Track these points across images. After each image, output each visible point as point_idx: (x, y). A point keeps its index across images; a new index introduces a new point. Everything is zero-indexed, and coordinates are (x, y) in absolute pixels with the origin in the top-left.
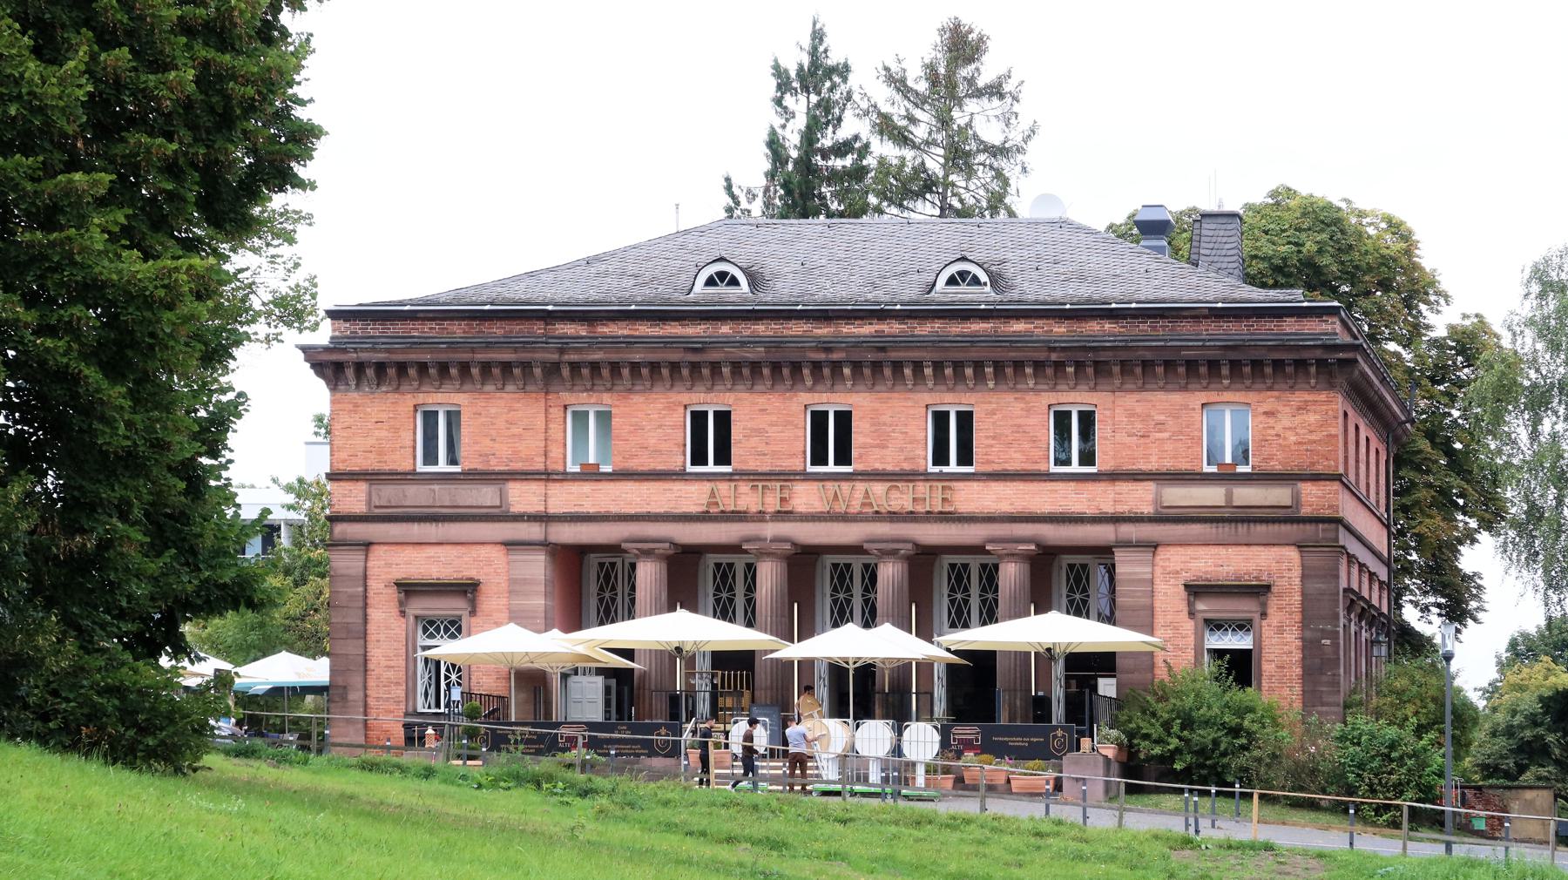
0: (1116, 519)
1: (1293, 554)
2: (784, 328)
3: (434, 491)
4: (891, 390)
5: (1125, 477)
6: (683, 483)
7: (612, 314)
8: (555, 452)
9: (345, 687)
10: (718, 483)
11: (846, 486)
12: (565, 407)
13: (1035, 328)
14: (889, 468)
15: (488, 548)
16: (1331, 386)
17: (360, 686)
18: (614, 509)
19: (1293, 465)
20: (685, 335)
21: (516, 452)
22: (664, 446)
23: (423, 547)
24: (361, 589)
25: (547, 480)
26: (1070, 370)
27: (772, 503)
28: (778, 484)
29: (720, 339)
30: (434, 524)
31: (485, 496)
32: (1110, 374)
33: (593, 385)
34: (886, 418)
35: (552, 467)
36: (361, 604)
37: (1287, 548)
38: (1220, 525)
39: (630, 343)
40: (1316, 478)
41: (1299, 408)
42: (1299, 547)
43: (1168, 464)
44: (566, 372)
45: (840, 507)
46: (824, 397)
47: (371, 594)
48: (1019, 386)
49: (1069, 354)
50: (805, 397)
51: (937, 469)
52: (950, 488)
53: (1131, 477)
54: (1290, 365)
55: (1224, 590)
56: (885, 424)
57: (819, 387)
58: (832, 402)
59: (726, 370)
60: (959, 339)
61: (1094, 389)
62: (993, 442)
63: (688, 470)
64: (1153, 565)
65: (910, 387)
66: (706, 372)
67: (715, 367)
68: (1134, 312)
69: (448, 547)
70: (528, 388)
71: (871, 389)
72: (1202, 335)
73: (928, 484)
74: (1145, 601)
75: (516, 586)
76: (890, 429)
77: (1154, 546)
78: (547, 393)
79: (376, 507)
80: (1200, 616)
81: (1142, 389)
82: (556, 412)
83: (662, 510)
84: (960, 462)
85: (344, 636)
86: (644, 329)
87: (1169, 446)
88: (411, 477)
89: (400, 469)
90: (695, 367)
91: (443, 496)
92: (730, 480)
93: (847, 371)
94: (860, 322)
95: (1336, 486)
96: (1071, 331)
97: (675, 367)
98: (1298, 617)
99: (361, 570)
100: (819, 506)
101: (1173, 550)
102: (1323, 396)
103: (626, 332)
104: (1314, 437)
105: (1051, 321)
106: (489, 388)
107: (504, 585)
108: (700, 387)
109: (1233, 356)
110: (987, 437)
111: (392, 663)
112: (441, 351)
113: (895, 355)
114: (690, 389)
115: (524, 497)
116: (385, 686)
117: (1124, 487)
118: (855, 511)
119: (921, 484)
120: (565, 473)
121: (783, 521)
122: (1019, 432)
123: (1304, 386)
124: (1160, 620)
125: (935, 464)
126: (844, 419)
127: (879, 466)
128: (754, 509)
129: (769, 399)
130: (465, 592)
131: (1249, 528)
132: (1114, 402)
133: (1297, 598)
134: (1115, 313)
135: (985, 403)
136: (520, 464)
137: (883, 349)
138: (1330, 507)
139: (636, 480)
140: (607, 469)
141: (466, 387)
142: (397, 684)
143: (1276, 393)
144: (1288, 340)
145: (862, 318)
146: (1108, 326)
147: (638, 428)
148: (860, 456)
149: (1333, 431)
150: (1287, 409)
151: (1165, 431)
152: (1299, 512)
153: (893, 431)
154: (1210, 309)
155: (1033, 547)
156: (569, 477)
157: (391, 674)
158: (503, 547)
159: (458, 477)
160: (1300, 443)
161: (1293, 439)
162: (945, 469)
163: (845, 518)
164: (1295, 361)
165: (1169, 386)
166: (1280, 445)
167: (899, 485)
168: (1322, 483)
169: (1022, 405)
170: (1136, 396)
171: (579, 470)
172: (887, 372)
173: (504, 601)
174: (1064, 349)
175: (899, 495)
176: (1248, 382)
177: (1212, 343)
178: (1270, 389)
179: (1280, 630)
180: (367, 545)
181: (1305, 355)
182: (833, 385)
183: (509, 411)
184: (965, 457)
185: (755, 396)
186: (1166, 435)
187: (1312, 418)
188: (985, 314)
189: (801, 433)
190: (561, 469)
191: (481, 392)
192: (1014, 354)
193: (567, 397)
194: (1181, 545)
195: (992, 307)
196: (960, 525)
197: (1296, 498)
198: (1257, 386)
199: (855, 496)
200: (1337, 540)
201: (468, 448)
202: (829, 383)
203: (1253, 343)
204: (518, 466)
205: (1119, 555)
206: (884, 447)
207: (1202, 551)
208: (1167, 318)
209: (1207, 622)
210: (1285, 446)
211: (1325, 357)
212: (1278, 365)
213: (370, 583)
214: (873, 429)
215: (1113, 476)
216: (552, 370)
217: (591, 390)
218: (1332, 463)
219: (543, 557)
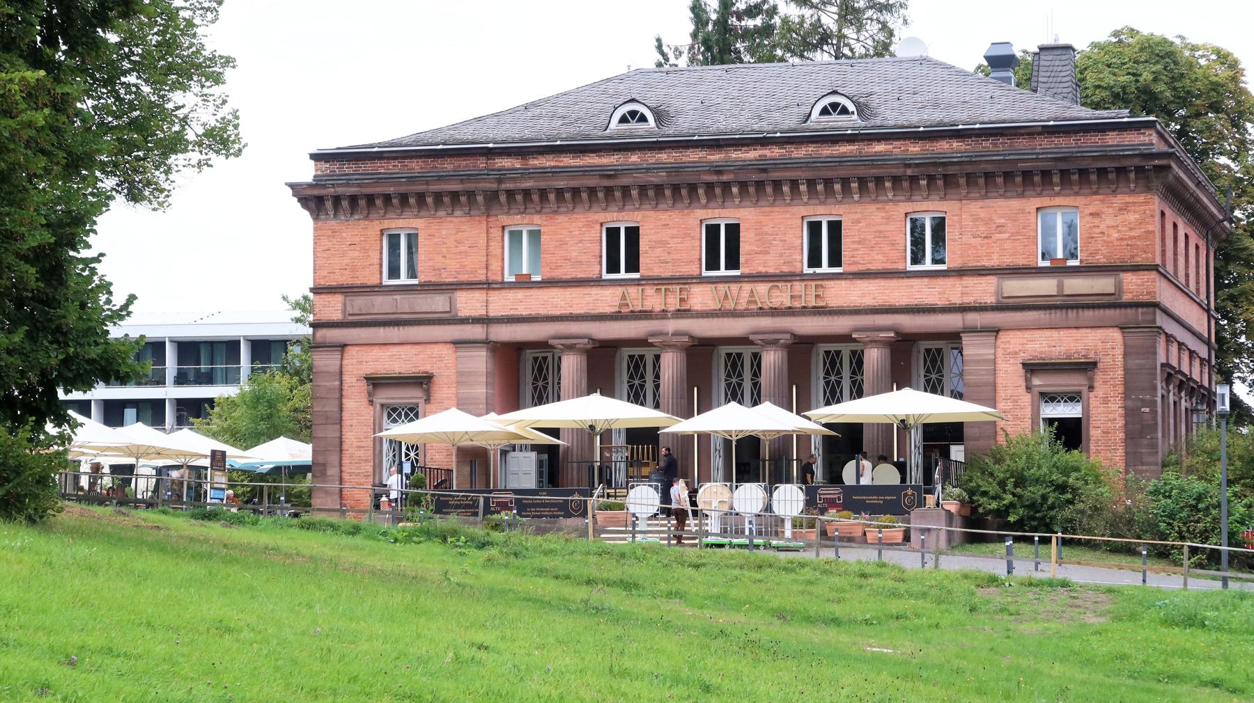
0: (963, 309)
1: (1116, 335)
2: (683, 156)
3: (396, 299)
4: (772, 205)
5: (970, 273)
6: (599, 288)
7: (541, 149)
8: (495, 265)
9: (324, 465)
10: (628, 288)
11: (734, 287)
12: (503, 228)
13: (894, 148)
14: (771, 270)
15: (440, 347)
16: (1148, 189)
17: (337, 463)
19: (1116, 258)
20: (600, 164)
21: (463, 266)
22: (584, 258)
23: (388, 347)
24: (337, 383)
25: (489, 289)
26: (923, 183)
27: (673, 303)
28: (678, 287)
29: (630, 167)
30: (396, 328)
31: (438, 303)
32: (958, 186)
33: (526, 208)
34: (768, 229)
35: (492, 278)
36: (337, 396)
37: (1111, 330)
38: (1053, 311)
39: (556, 172)
40: (1136, 268)
41: (1121, 209)
42: (1121, 328)
43: (1008, 261)
44: (503, 198)
45: (730, 305)
46: (717, 212)
47: (345, 387)
48: (880, 198)
49: (922, 169)
50: (700, 213)
51: (811, 271)
52: (822, 286)
53: (976, 272)
54: (1112, 172)
55: (1057, 367)
56: (767, 234)
57: (712, 204)
58: (722, 217)
59: (634, 193)
60: (829, 160)
61: (943, 198)
63: (604, 277)
64: (995, 348)
65: (788, 202)
66: (618, 194)
67: (626, 190)
68: (977, 132)
69: (409, 347)
70: (473, 212)
71: (756, 204)
72: (1035, 149)
73: (803, 284)
74: (991, 378)
75: (463, 378)
76: (772, 238)
77: (996, 331)
78: (488, 216)
79: (350, 315)
80: (1036, 390)
81: (985, 197)
82: (496, 232)
83: (582, 312)
84: (831, 265)
85: (324, 422)
86: (567, 161)
87: (1008, 245)
88: (378, 289)
89: (369, 283)
90: (609, 191)
91: (404, 304)
92: (638, 285)
93: (735, 190)
94: (746, 148)
95: (1153, 275)
96: (924, 150)
97: (592, 191)
98: (1121, 389)
99: (338, 367)
100: (712, 305)
101: (1012, 334)
102: (1141, 198)
103: (552, 164)
104: (1133, 234)
105: (907, 142)
106: (441, 213)
107: (453, 378)
108: (613, 207)
109: (1063, 166)
110: (854, 242)
111: (363, 444)
112: (400, 184)
113: (775, 175)
114: (605, 210)
115: (469, 303)
116: (357, 463)
117: (969, 281)
118: (743, 308)
119: (797, 283)
120: (503, 283)
121: (683, 318)
122: (880, 237)
123: (1125, 189)
124: (1001, 394)
125: (810, 266)
126: (733, 230)
127: (762, 269)
128: (658, 308)
129: (671, 216)
130: (422, 383)
131: (1077, 313)
132: (961, 209)
133: (1120, 372)
134: (962, 133)
136: (466, 276)
137: (765, 171)
138: (1148, 293)
139: (561, 287)
140: (537, 278)
141: (422, 213)
142: (367, 461)
143: (1101, 197)
144: (1110, 151)
145: (748, 145)
146: (956, 144)
147: (563, 243)
148: (747, 262)
149: (1150, 228)
150: (1111, 210)
151: (1005, 232)
152: (1121, 298)
154: (1043, 126)
155: (892, 335)
156: (506, 286)
157: (361, 453)
159: (416, 288)
160: (1122, 239)
161: (1116, 235)
162: (818, 270)
163: (734, 314)
164: (1116, 168)
165: (1009, 194)
166: (1105, 241)
167: (779, 284)
168: (1142, 273)
169: (884, 214)
170: (980, 203)
171: (514, 280)
172: (769, 189)
173: (453, 390)
174: (917, 165)
175: (779, 294)
176: (1076, 188)
177: (1044, 156)
178: (1096, 193)
179: (1106, 401)
180: (343, 347)
181: (1126, 163)
182: (724, 202)
183: (457, 232)
184: (835, 260)
185: (659, 213)
186: (1006, 236)
187: (1132, 217)
188: (851, 138)
189: (697, 243)
190: (499, 279)
191: (434, 217)
192: (875, 171)
193: (504, 219)
194: (1019, 329)
195: (857, 132)
196: (830, 318)
197: (1119, 286)
198: (1083, 191)
199: (742, 295)
200: (1154, 321)
201: (424, 264)
202: (720, 201)
203: (1079, 155)
204: (464, 278)
205: (966, 339)
206: (767, 253)
207: (1037, 334)
208: (1007, 136)
209: (1043, 395)
210: (1108, 242)
211: (1143, 164)
212: (1102, 172)
213: (345, 378)
214: (757, 238)
215: (960, 273)
216: (492, 197)
217: (523, 213)
218: (1150, 255)
219: (485, 353)
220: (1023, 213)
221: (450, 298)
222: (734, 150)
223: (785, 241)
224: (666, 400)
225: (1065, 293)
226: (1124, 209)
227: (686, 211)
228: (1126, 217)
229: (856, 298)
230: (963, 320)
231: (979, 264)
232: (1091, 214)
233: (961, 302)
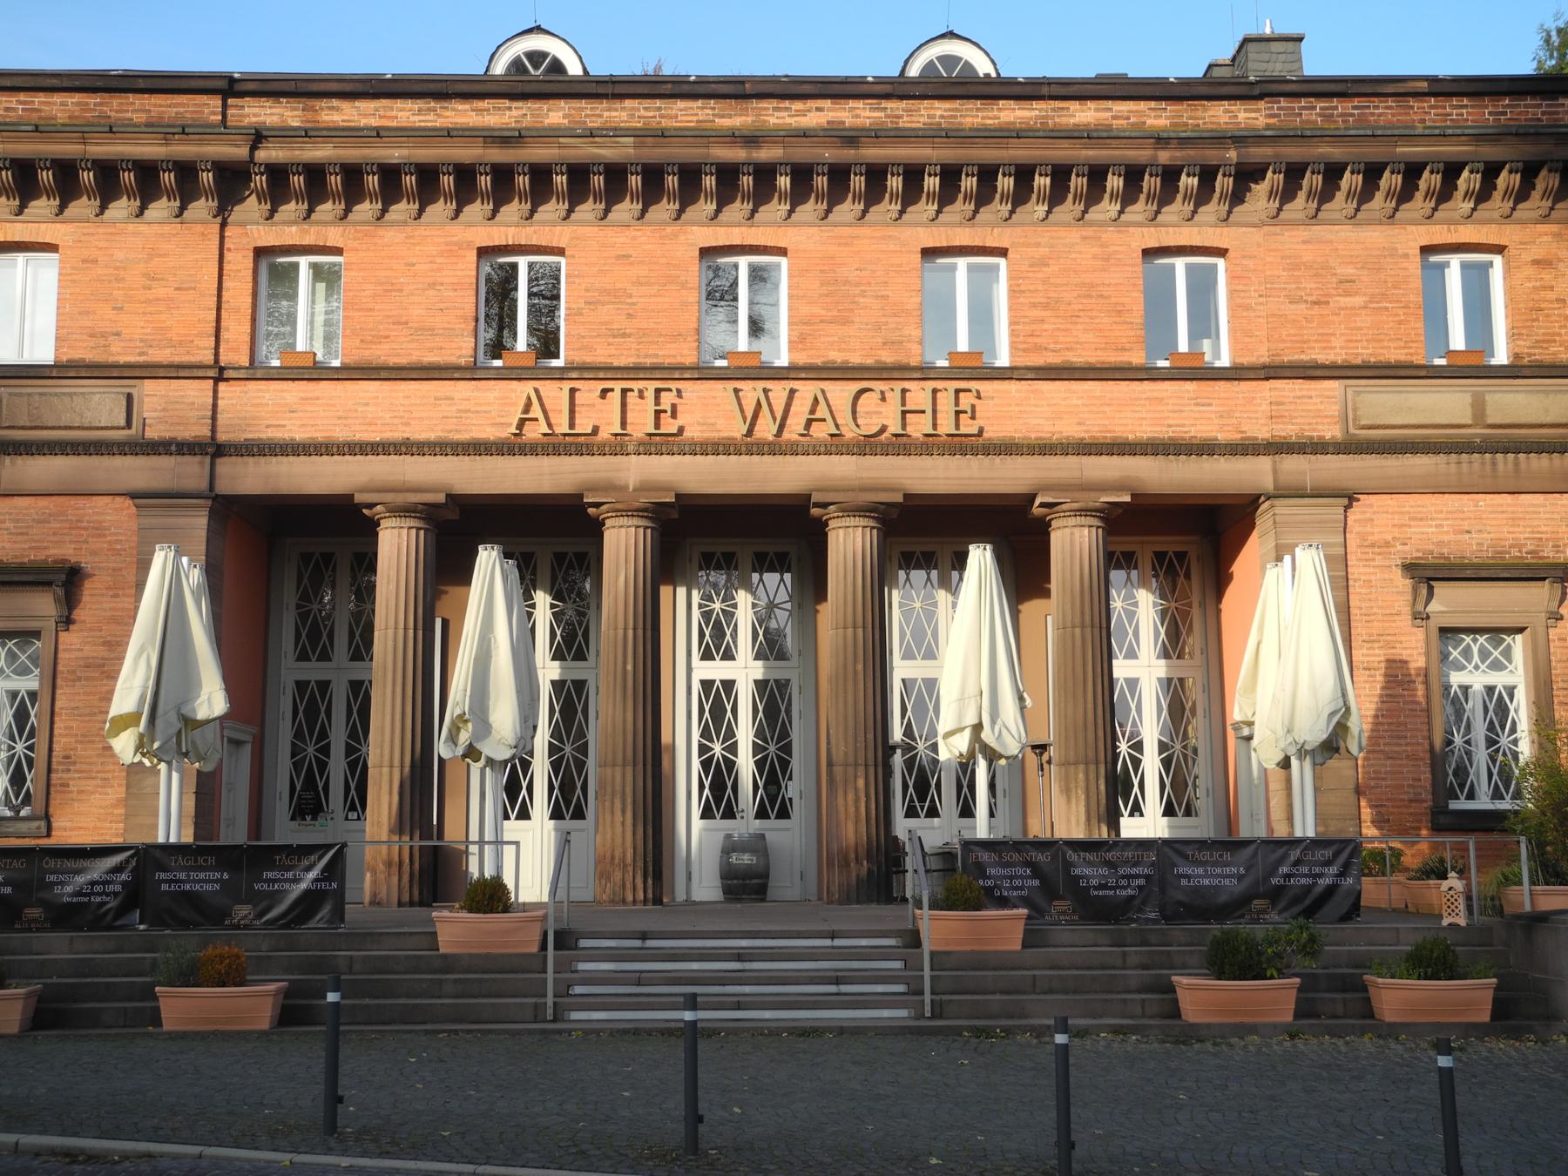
2: (662, 116)
14: (856, 359)
18: (341, 434)
43: (1364, 352)
56: (846, 282)
62: (1043, 313)
76: (857, 291)
80: (1435, 623)
83: (432, 436)
86: (405, 113)
110: (1034, 305)
122: (1090, 296)
127: (836, 357)
129: (634, 238)
135: (1028, 245)
136: (168, 351)
151: (1356, 294)
153: (863, 294)
158: (129, 502)
170: (1303, 233)
185: (609, 232)
186: (1358, 300)
206: (846, 322)
214: (824, 290)
220: (1391, 256)
221: (129, 398)
222: (775, 109)
223: (886, 297)
225: (1490, 421)
229: (1042, 422)
230: (1275, 471)
231: (1303, 357)
232: (1536, 262)
233: (1267, 435)
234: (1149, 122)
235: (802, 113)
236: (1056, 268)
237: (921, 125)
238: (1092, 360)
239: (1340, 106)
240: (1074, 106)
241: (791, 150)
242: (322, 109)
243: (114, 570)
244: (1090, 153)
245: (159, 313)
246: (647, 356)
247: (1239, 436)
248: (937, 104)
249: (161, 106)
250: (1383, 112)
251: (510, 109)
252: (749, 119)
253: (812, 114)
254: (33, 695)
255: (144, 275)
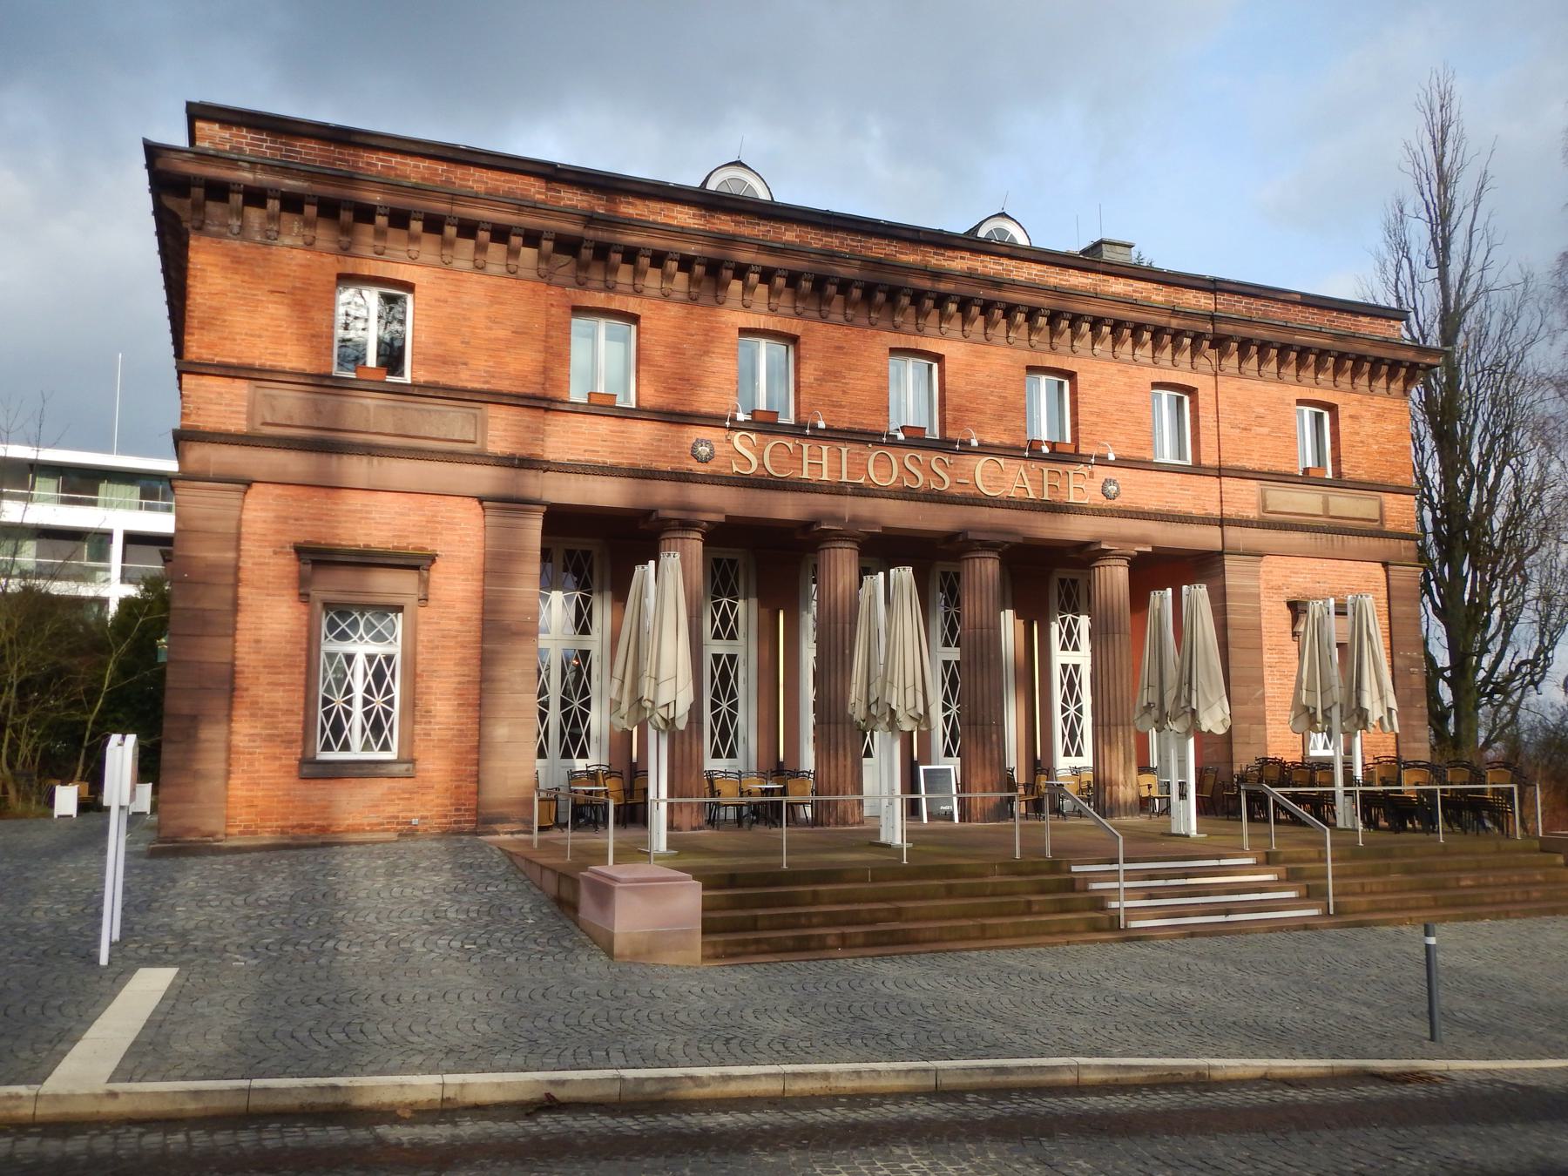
13: (1134, 291)
43: (1269, 464)
76: (987, 391)
99: (234, 523)
110: (1092, 413)
129: (846, 335)
136: (507, 382)
186: (1265, 430)
213: (246, 545)
222: (935, 254)
223: (1005, 397)
224: (840, 626)
225: (1331, 514)
226: (1380, 416)
227: (869, 331)
228: (1384, 425)
231: (1238, 464)
232: (1351, 417)
234: (1154, 297)
235: (952, 259)
236: (1104, 389)
237: (1023, 279)
238: (1125, 454)
239: (1257, 304)
240: (1112, 279)
241: (960, 286)
242: (621, 202)
243: (464, 558)
244: (1134, 314)
245: (499, 350)
246: (856, 423)
247: (1203, 512)
248: (1033, 266)
249: (497, 180)
250: (1276, 311)
251: (759, 224)
252: (919, 258)
253: (958, 260)
254: (389, 659)
255: (488, 318)
